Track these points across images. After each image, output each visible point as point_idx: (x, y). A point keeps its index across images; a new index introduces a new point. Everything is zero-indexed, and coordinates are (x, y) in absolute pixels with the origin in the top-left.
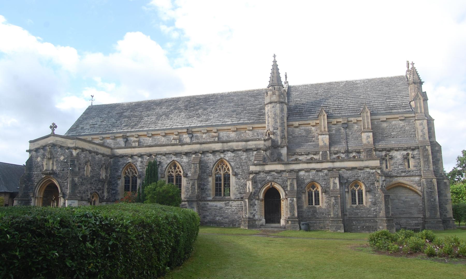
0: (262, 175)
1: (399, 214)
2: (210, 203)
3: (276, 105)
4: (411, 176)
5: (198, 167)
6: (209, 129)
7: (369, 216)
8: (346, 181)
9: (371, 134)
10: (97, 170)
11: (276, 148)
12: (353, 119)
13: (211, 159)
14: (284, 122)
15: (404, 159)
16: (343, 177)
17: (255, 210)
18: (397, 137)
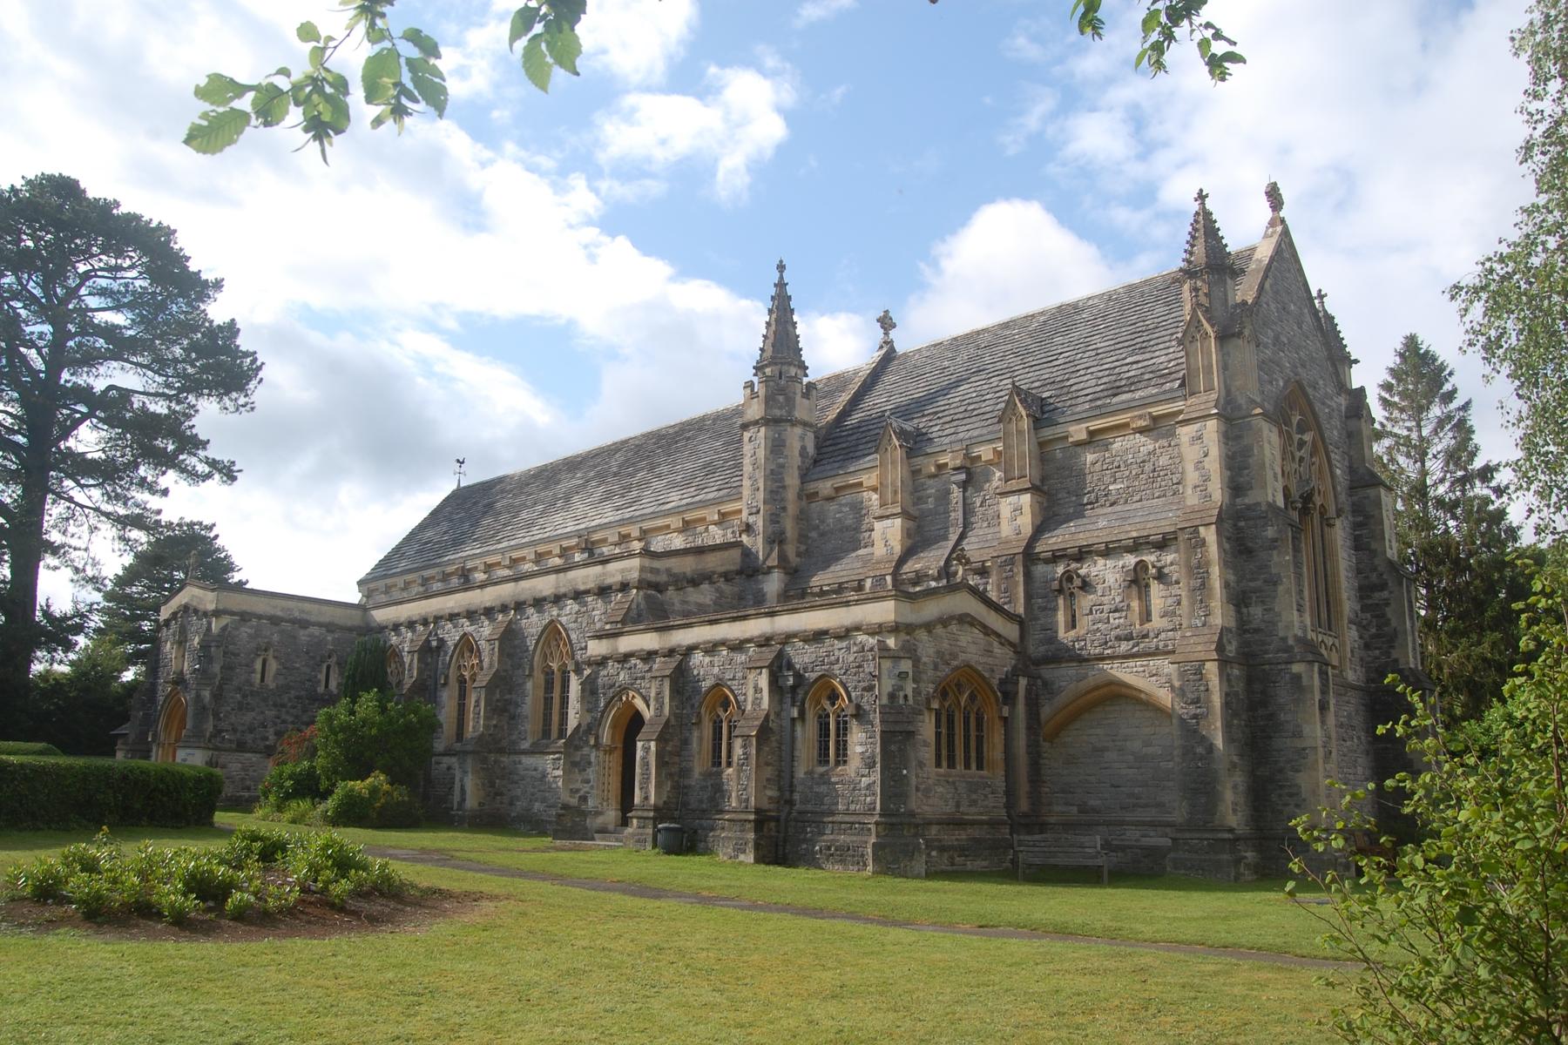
0: (612, 667)
1: (1122, 808)
2: (527, 761)
3: (759, 431)
4: (1149, 654)
5: (496, 650)
6: (624, 530)
7: (852, 807)
8: (791, 681)
9: (1026, 499)
10: (307, 670)
11: (752, 576)
12: (985, 452)
13: (533, 623)
14: (784, 487)
15: (1129, 587)
16: (790, 666)
17: (588, 781)
18: (1126, 502)
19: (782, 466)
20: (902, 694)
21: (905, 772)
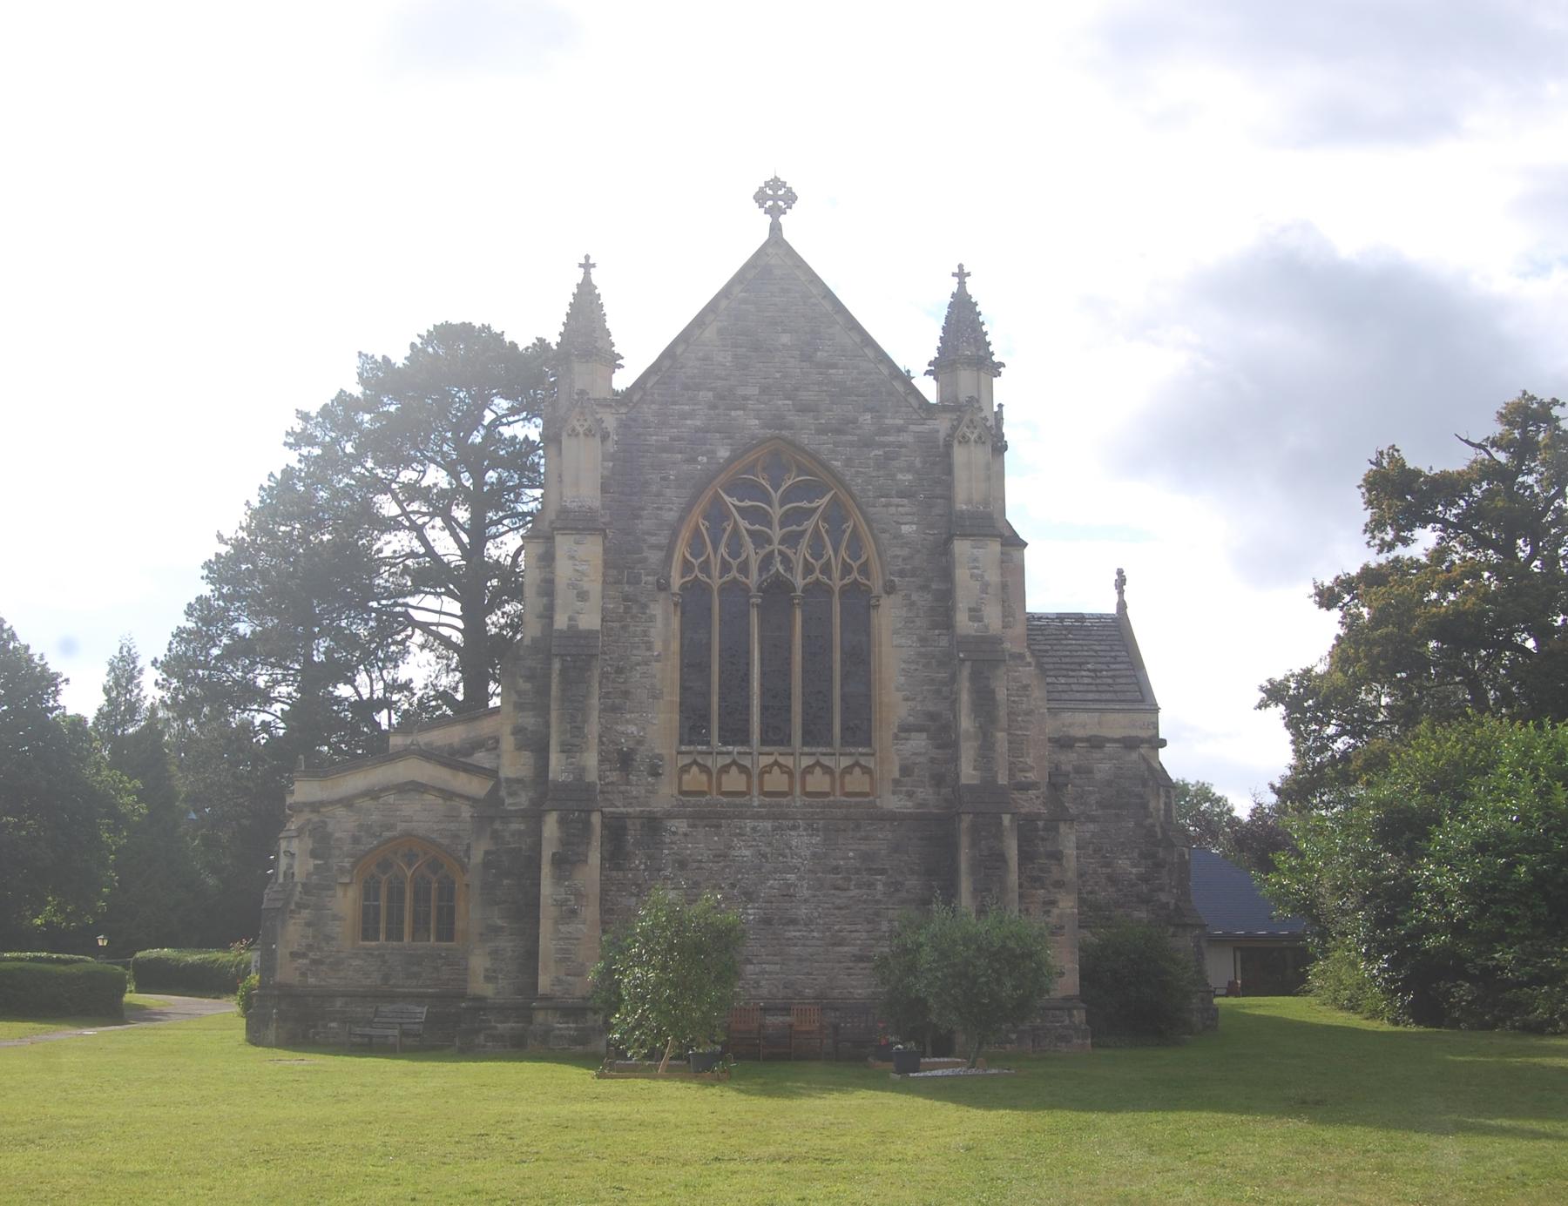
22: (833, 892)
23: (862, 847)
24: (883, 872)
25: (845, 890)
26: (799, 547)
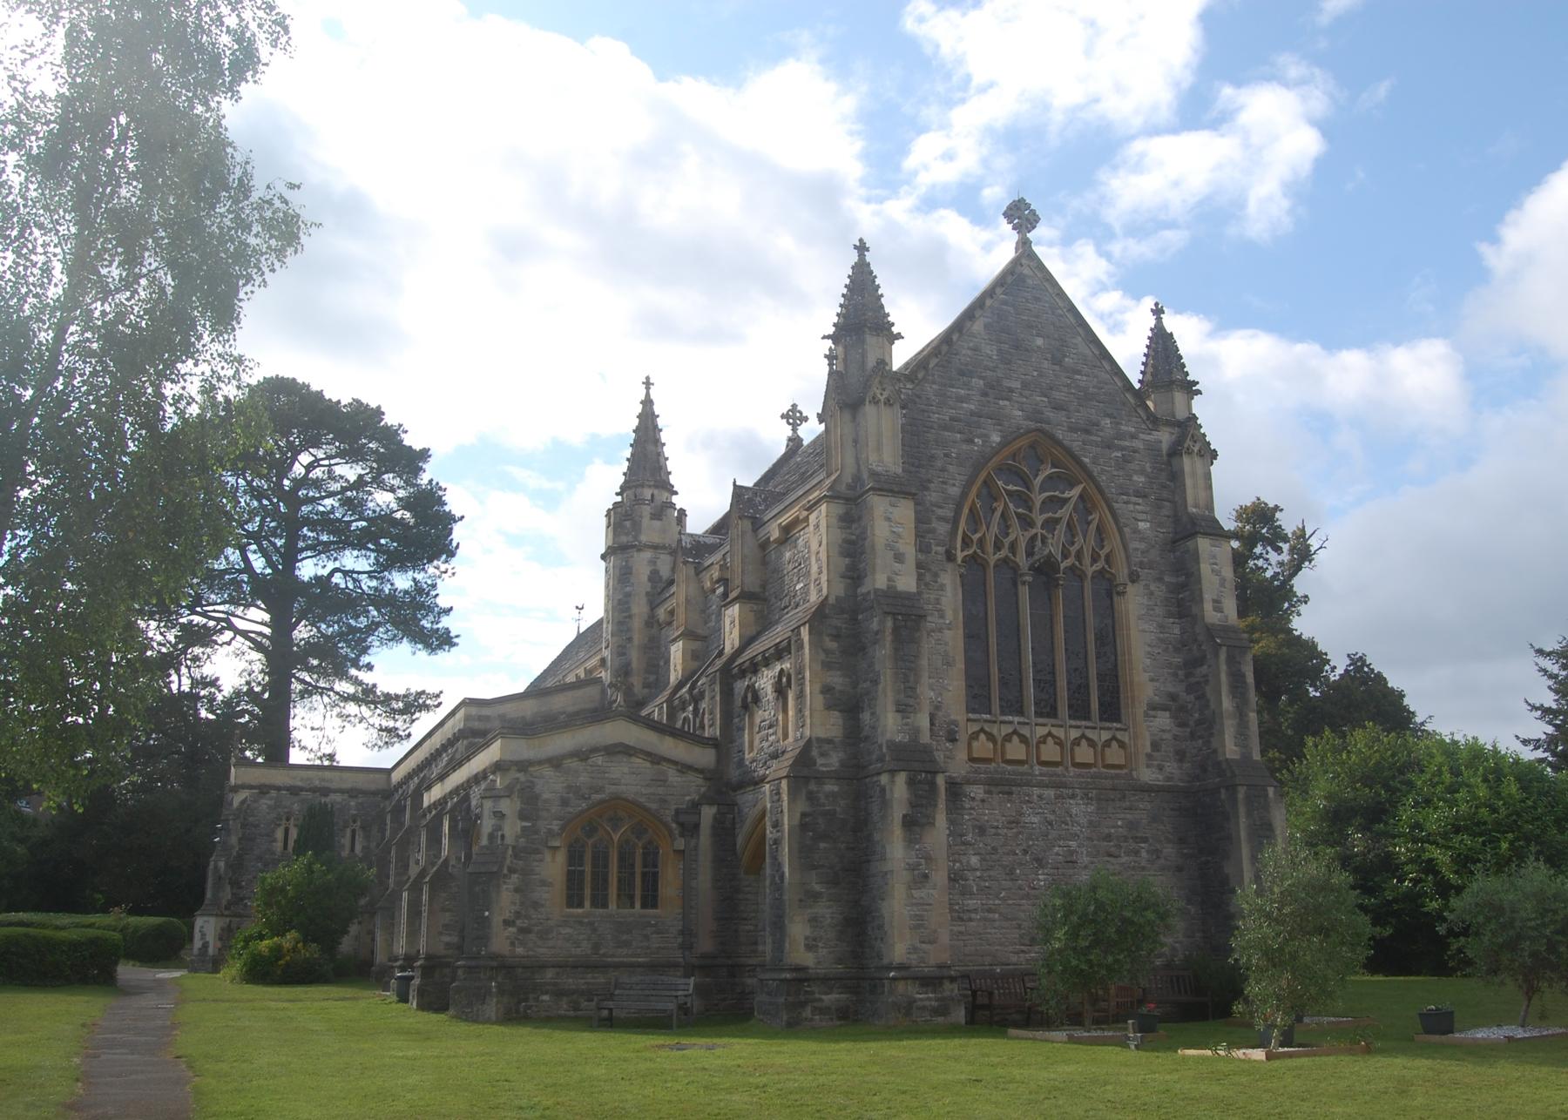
19: (628, 595)
20: (500, 833)
21: (487, 913)
22: (1107, 858)
23: (1128, 816)
24: (1145, 840)
25: (1116, 857)
26: (1056, 533)
